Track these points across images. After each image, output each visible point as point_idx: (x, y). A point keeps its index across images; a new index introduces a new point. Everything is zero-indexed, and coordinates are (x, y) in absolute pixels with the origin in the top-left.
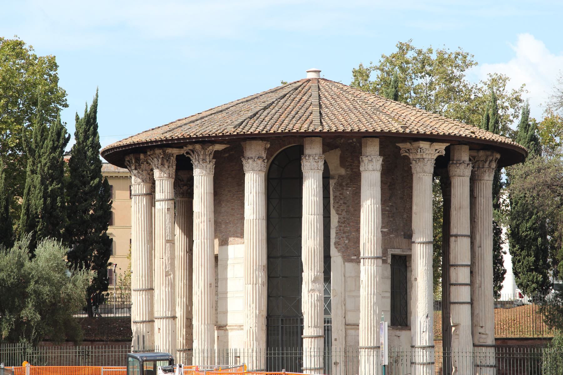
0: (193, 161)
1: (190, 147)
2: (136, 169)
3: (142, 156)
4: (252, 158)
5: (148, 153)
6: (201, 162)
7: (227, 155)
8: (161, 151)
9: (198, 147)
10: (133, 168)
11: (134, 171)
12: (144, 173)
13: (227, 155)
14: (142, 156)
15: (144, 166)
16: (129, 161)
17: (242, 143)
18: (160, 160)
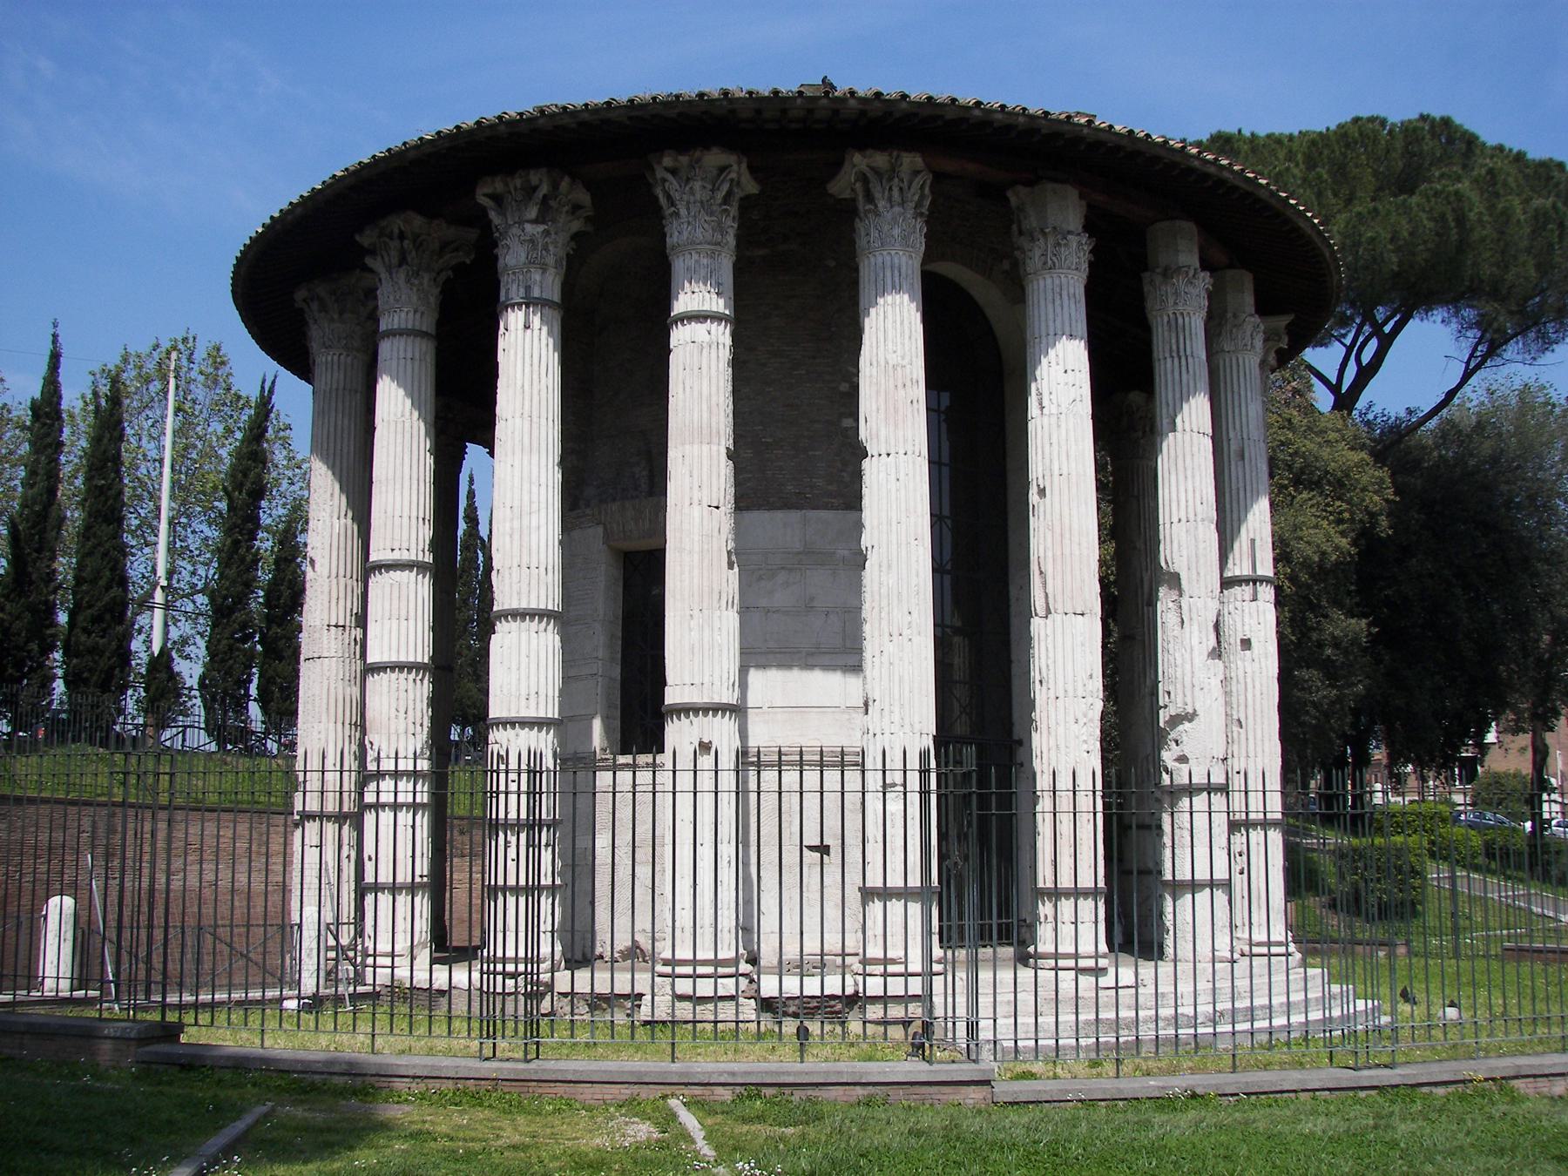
0: (881, 204)
1: (881, 160)
2: (536, 221)
3: (565, 184)
4: (1069, 232)
5: (667, 161)
6: (910, 213)
7: (761, 252)
8: (731, 159)
9: (910, 161)
10: (533, 212)
11: (528, 227)
12: (563, 238)
13: (761, 252)
14: (565, 184)
15: (562, 218)
16: (498, 199)
17: (1023, 190)
18: (725, 187)
